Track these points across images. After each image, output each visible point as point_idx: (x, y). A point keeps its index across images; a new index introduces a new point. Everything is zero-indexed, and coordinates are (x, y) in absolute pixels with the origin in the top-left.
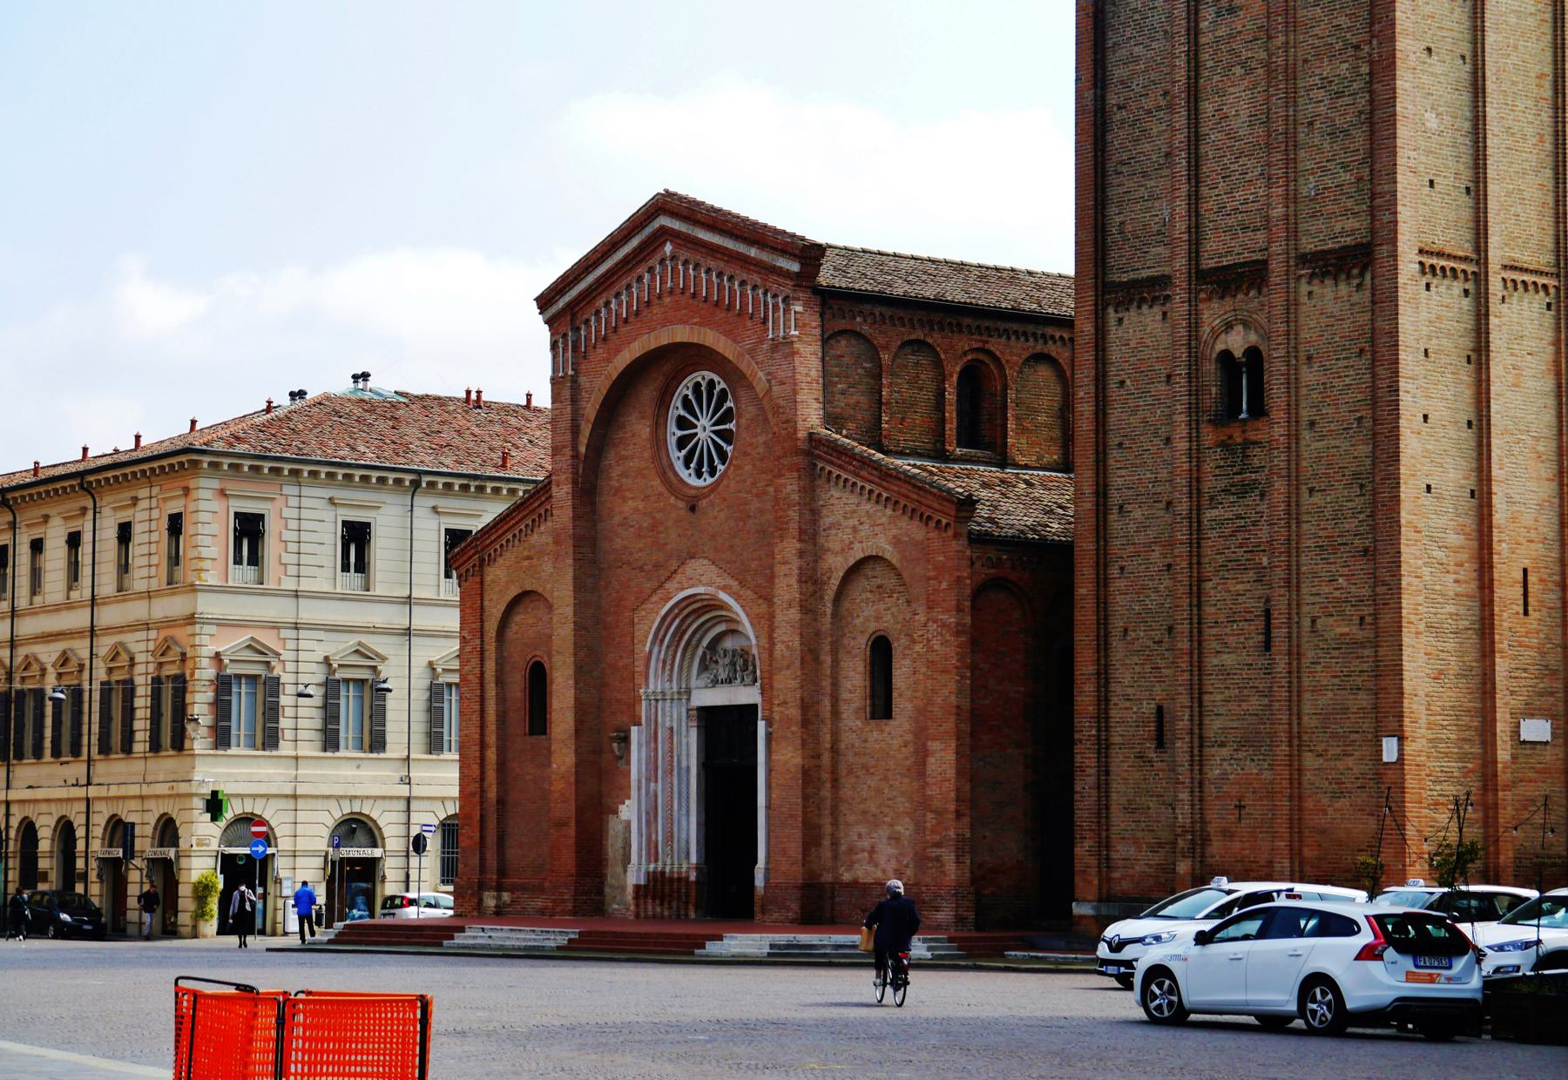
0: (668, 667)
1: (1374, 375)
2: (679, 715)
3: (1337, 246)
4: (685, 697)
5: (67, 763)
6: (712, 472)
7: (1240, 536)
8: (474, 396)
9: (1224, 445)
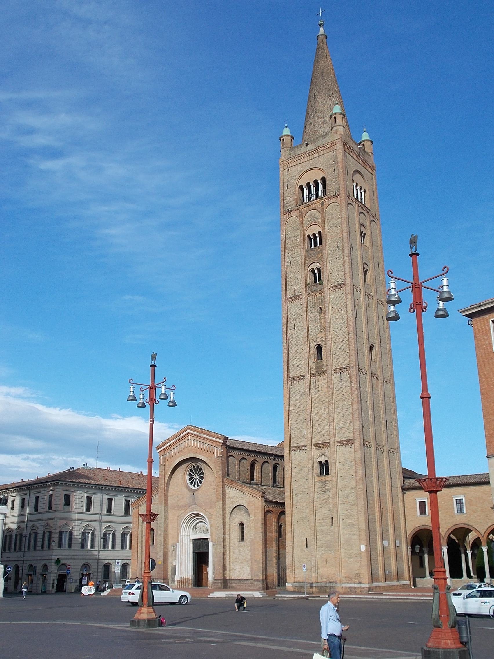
1: (355, 467)
3: (345, 439)
5: (18, 552)
6: (198, 486)
7: (325, 501)
8: (109, 469)
9: (321, 481)
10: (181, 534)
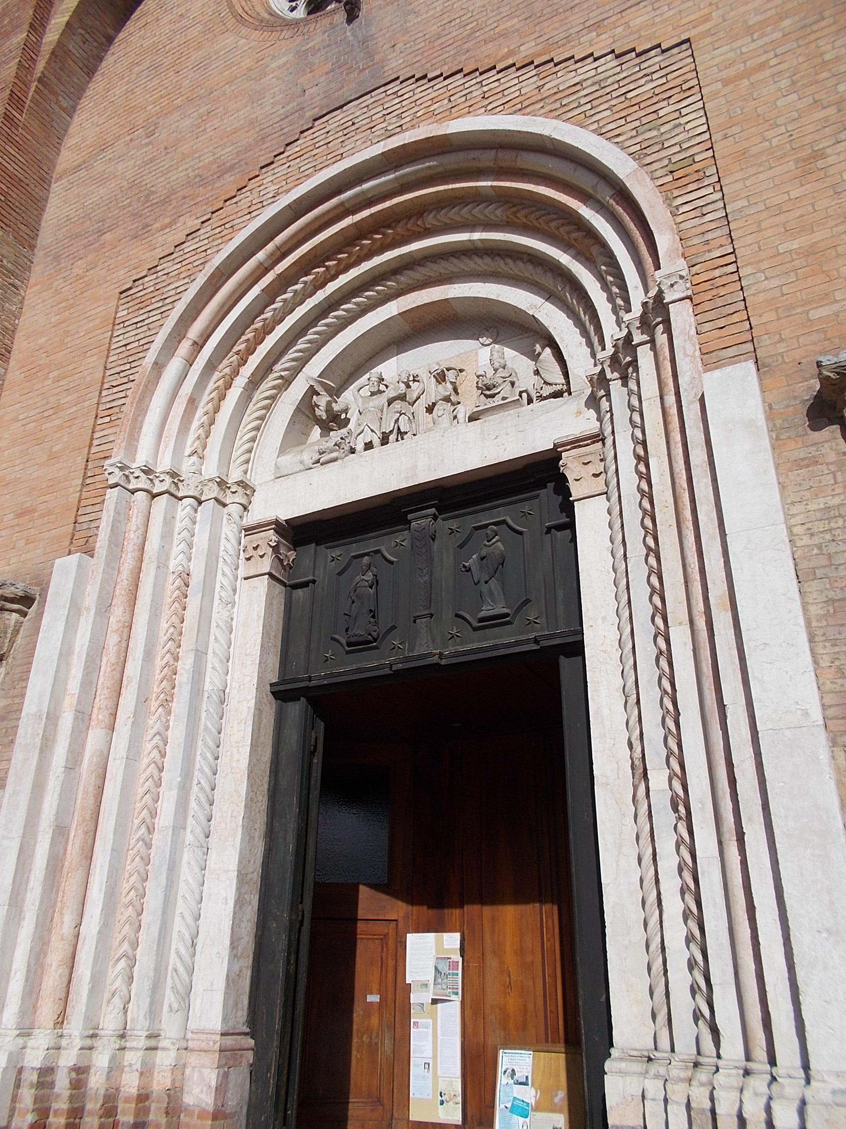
0: (199, 417)
2: (214, 540)
4: (240, 498)
10: (142, 458)
